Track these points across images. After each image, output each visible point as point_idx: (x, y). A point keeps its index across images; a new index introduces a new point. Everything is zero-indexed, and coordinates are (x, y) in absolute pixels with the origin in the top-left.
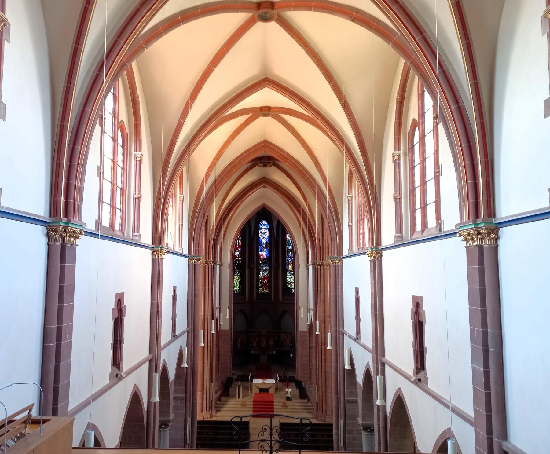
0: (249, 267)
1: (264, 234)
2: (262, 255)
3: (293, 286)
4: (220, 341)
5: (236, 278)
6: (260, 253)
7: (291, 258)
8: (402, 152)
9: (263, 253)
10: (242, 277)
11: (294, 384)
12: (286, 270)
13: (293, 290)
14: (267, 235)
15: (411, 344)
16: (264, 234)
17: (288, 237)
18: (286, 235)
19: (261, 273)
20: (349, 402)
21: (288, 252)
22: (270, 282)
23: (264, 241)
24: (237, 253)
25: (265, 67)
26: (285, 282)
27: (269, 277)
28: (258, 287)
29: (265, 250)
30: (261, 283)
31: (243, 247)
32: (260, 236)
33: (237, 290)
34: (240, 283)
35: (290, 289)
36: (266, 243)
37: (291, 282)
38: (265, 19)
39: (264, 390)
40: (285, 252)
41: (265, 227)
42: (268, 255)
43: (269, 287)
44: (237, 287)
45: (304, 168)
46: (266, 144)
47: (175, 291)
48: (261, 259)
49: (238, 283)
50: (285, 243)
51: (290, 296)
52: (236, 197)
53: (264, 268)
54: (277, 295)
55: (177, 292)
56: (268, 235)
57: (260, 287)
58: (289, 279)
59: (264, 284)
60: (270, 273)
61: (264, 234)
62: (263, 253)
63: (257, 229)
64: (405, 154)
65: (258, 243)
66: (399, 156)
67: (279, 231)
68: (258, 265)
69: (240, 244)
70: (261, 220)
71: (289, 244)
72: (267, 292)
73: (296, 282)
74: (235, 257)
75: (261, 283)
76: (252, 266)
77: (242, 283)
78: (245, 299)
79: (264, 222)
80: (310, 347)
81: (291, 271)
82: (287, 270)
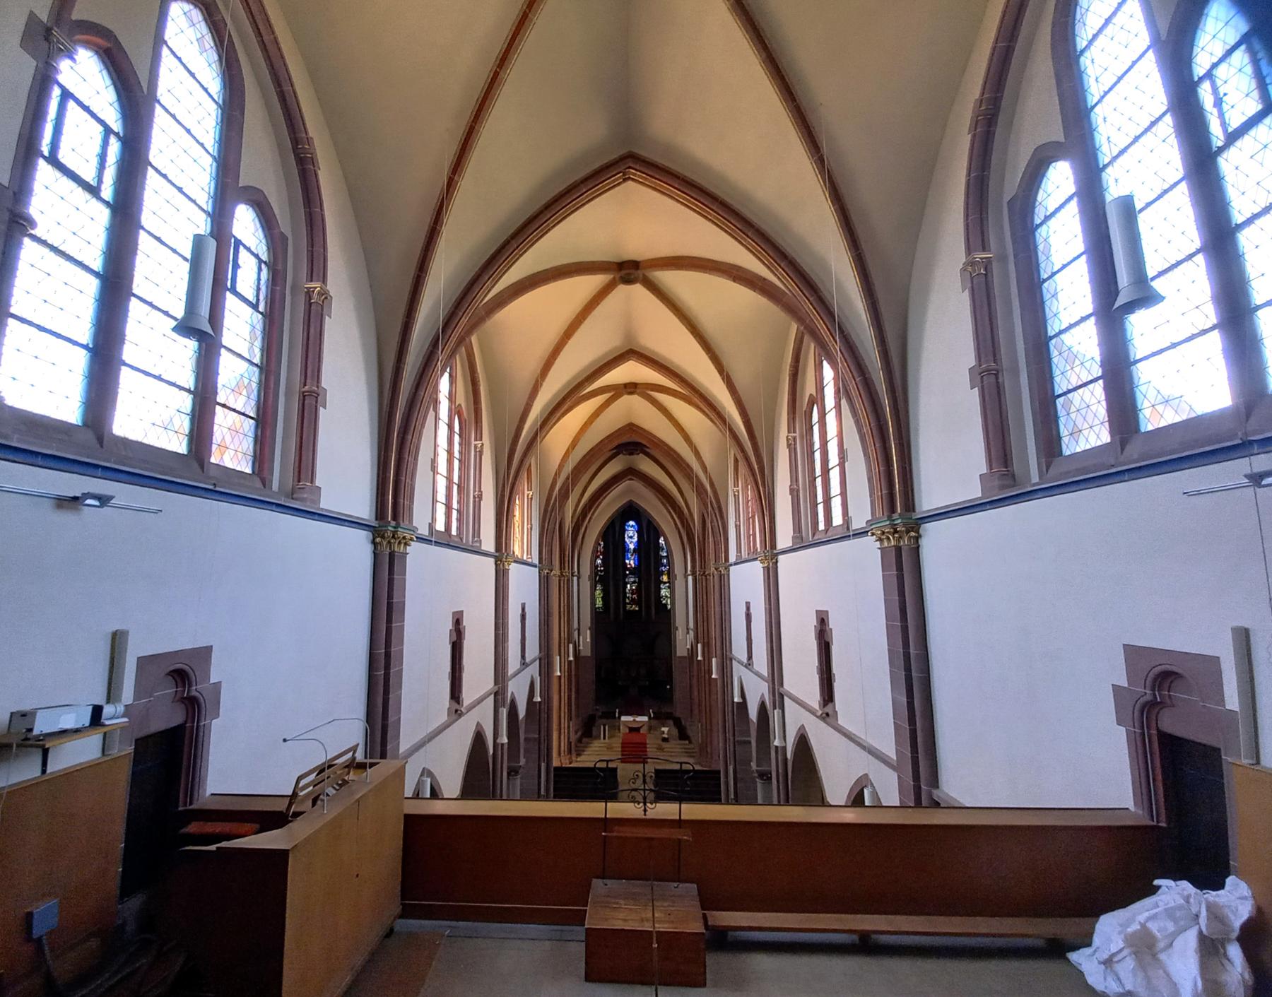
1: (631, 537)
5: (598, 592)
8: (797, 435)
9: (631, 562)
11: (671, 722)
14: (636, 539)
15: (815, 670)
17: (661, 541)
20: (741, 743)
23: (632, 547)
24: (599, 561)
25: (629, 335)
26: (659, 597)
28: (625, 604)
31: (605, 554)
32: (627, 540)
35: (666, 605)
38: (628, 281)
39: (634, 730)
44: (599, 603)
45: (678, 455)
46: (631, 427)
47: (523, 609)
50: (658, 547)
51: (665, 615)
55: (527, 610)
58: (663, 592)
59: (633, 600)
60: (639, 583)
61: (631, 537)
62: (631, 562)
63: (624, 531)
64: (802, 437)
66: (795, 439)
67: (649, 532)
73: (672, 597)
77: (605, 599)
79: (631, 523)
80: (691, 677)
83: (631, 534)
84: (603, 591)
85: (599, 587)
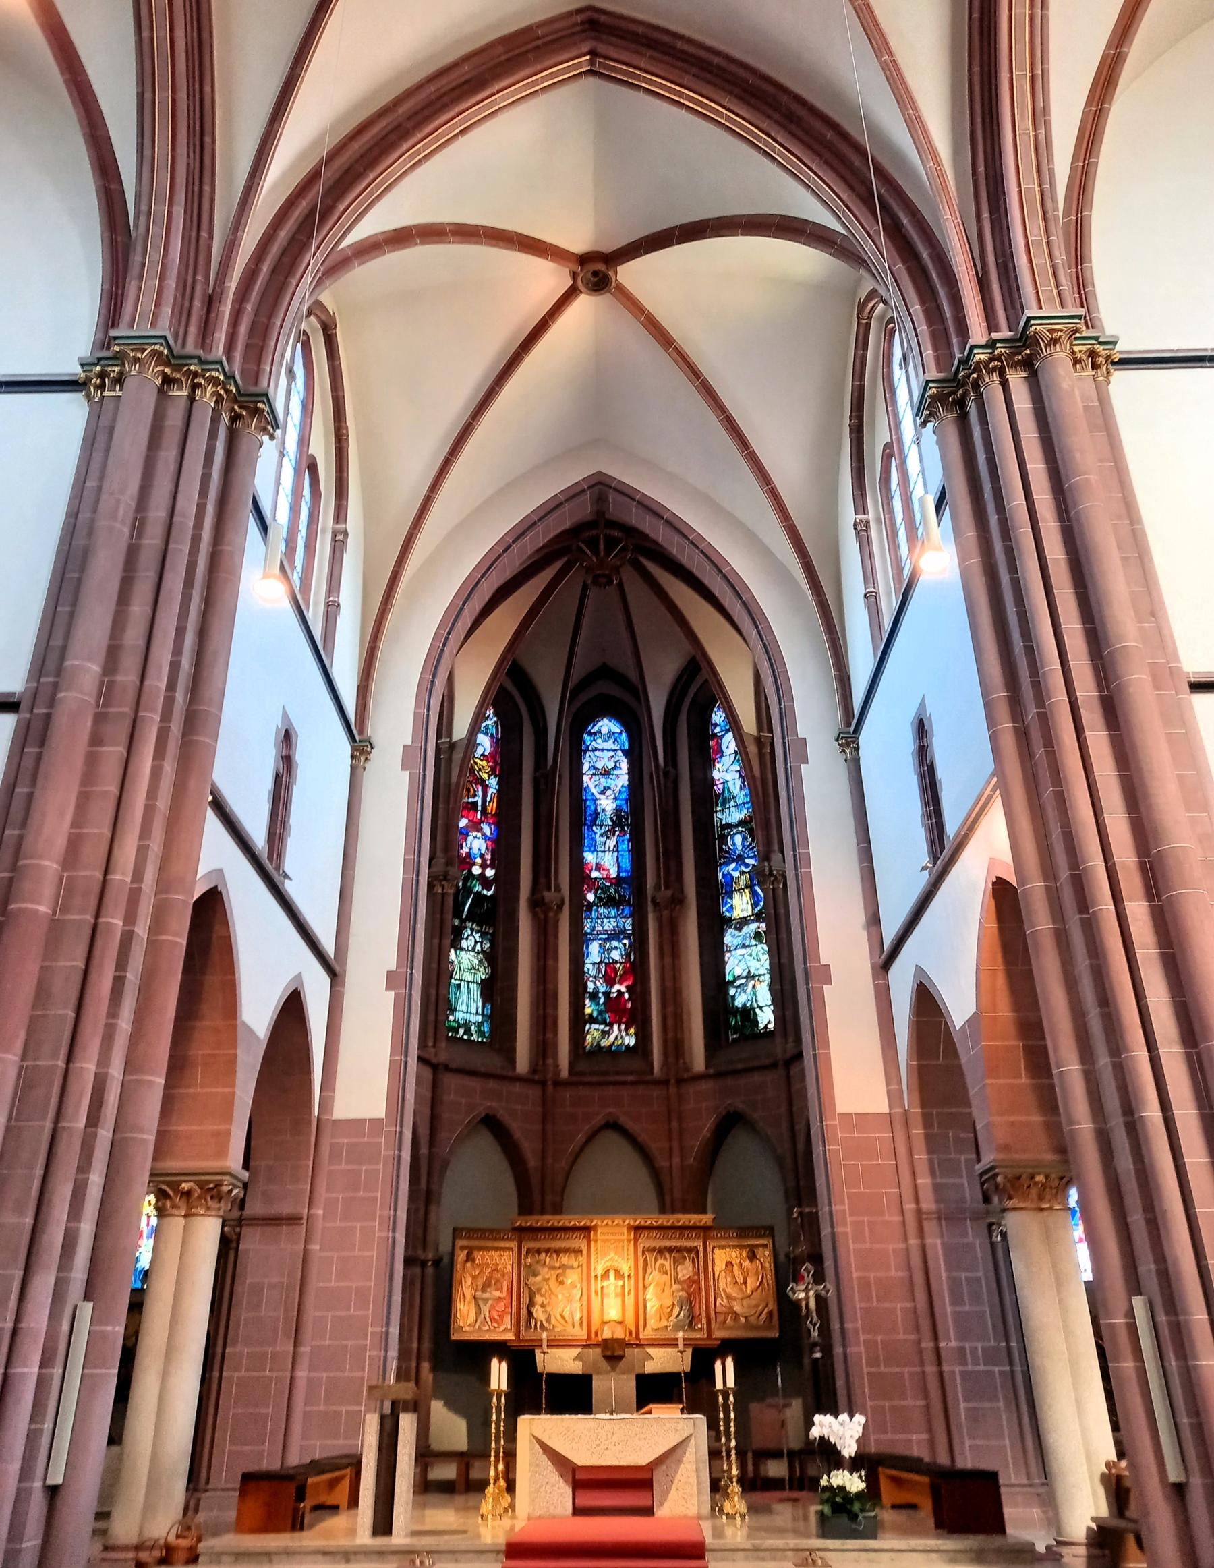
0: (536, 903)
2: (599, 867)
3: (764, 996)
4: (322, 1193)
5: (467, 961)
6: (589, 857)
7: (740, 859)
9: (606, 858)
10: (499, 963)
12: (715, 926)
13: (766, 1018)
14: (621, 779)
16: (606, 773)
17: (727, 773)
18: (705, 753)
19: (594, 948)
21: (723, 839)
22: (639, 991)
23: (607, 805)
24: (476, 844)
26: (716, 983)
27: (636, 968)
28: (579, 1021)
29: (612, 843)
30: (594, 996)
33: (467, 1026)
34: (488, 989)
35: (748, 1014)
36: (618, 810)
37: (750, 976)
40: (711, 844)
41: (610, 744)
42: (626, 864)
43: (636, 1017)
44: (468, 1007)
48: (592, 884)
49: (476, 990)
50: (707, 797)
52: (419, 87)
53: (609, 925)
54: (676, 1046)
56: (623, 780)
57: (592, 1020)
59: (613, 1004)
62: (606, 858)
63: (577, 751)
65: (581, 815)
68: (580, 910)
69: (492, 806)
70: (593, 718)
71: (726, 799)
72: (630, 1041)
74: (468, 861)
75: (594, 996)
76: (549, 896)
77: (496, 990)
78: (512, 1061)
79: (606, 725)
81: (744, 922)
82: (724, 923)
83: (604, 761)
84: (490, 958)
85: (471, 939)
